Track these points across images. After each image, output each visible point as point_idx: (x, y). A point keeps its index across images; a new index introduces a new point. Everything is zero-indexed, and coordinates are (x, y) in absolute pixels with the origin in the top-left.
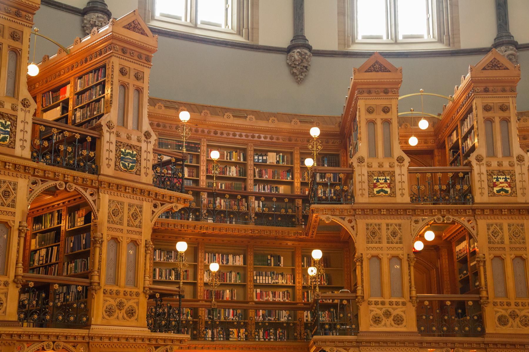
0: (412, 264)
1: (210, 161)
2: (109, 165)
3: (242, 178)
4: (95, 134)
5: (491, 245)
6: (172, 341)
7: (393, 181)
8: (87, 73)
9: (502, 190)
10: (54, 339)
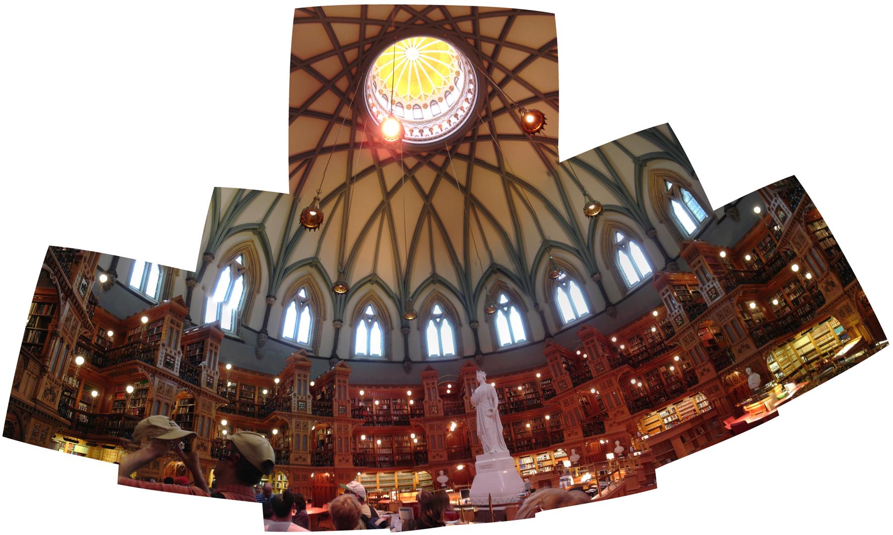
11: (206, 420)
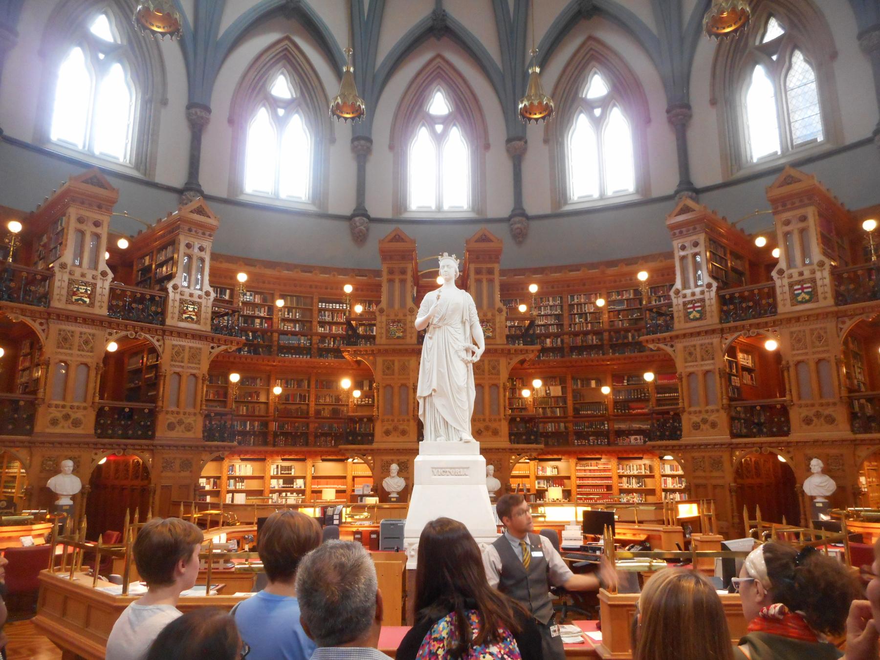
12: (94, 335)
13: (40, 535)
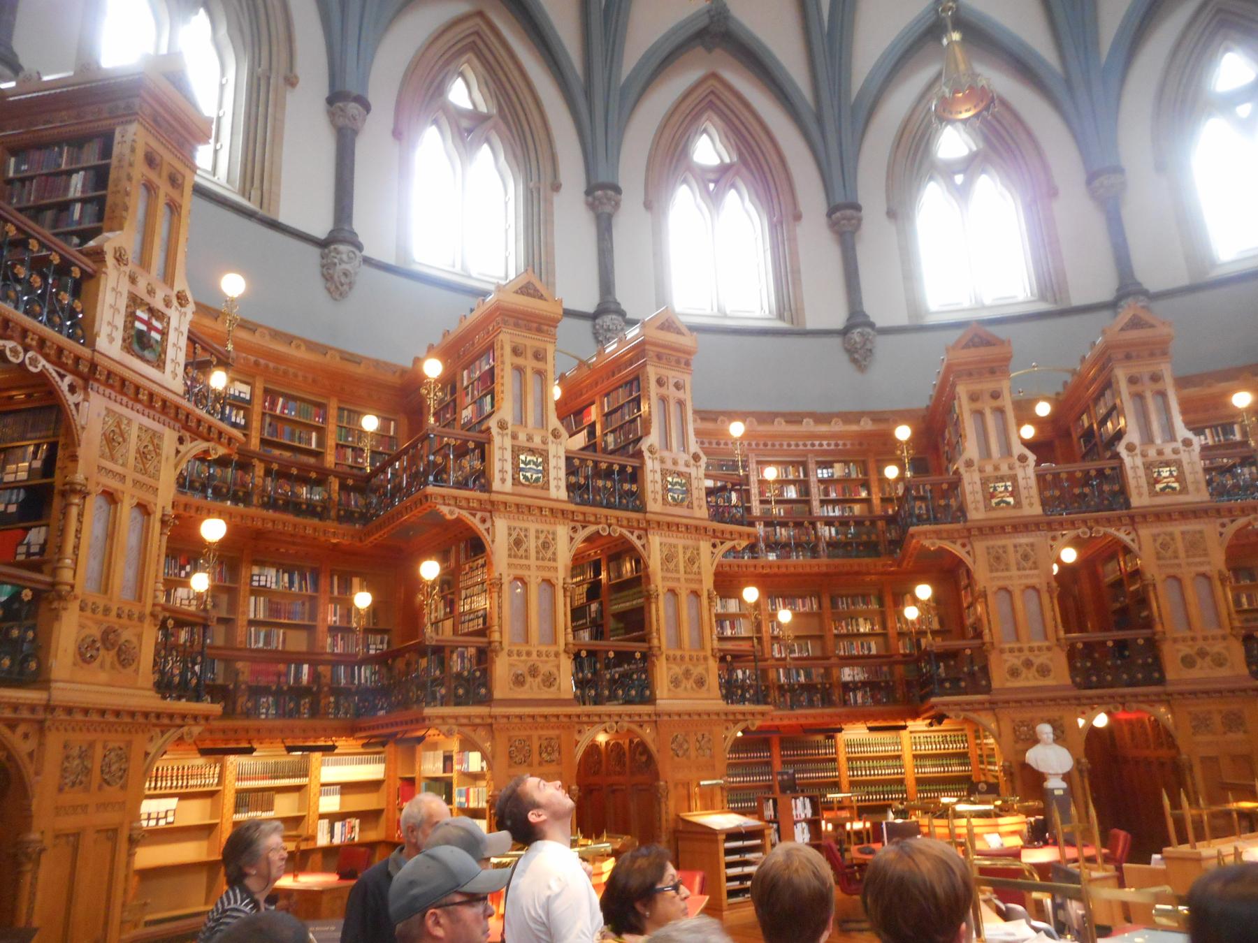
0: (1055, 595)
1: (763, 482)
2: (655, 500)
3: (804, 499)
4: (636, 463)
5: (1162, 562)
6: (753, 714)
7: (1015, 486)
8: (617, 388)
9: (1168, 487)
10: (616, 719)
11: (126, 511)
12: (1032, 545)
13: (1013, 833)
